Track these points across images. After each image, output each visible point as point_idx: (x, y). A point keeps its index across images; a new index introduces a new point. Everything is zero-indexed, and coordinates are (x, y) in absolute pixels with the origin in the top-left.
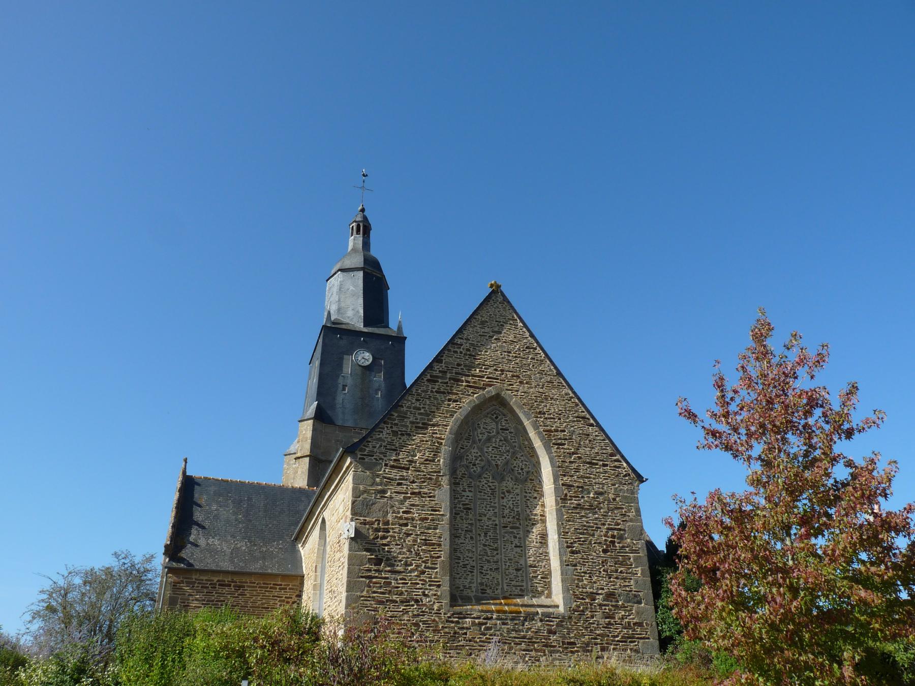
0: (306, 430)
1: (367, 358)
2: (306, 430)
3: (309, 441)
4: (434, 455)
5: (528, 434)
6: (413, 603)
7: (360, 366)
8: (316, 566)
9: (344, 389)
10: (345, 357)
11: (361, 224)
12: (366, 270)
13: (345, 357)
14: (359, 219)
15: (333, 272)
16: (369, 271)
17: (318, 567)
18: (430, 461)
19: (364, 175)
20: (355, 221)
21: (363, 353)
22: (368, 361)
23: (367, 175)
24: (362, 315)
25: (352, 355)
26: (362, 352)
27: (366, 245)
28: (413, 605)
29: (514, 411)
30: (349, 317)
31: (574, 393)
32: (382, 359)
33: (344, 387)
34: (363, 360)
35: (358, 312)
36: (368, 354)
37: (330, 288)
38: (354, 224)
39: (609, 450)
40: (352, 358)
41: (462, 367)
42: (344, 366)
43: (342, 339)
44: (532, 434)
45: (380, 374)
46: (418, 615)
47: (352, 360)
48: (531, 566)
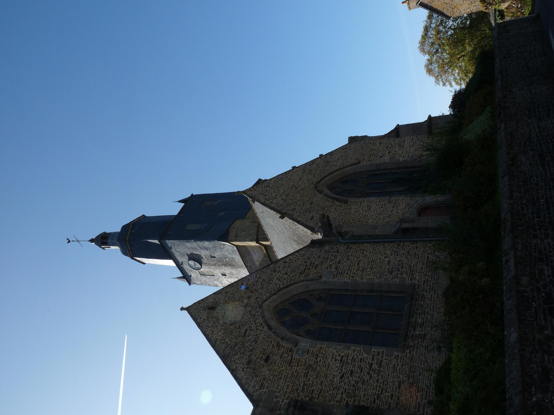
11: (103, 247)
12: (132, 255)
16: (131, 253)
20: (104, 249)
21: (191, 265)
23: (68, 239)
26: (191, 266)
43: (191, 275)
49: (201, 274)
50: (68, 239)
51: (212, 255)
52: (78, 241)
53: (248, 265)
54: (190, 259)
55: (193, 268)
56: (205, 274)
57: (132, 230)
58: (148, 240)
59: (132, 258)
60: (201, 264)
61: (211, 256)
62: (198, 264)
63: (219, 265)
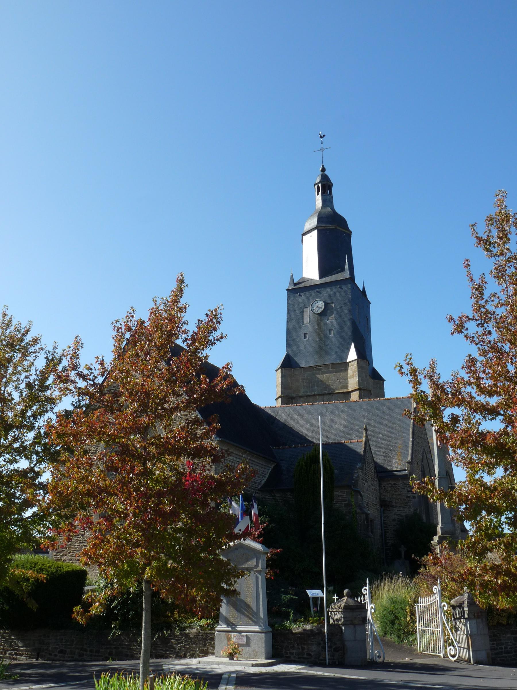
1: (320, 306)
4: (97, 449)
6: (81, 536)
9: (305, 337)
11: (320, 185)
12: (319, 228)
14: (318, 180)
18: (94, 453)
19: (321, 137)
20: (315, 184)
21: (317, 302)
22: (321, 308)
23: (324, 136)
26: (316, 302)
27: (327, 200)
28: (80, 537)
32: (332, 303)
34: (318, 308)
36: (321, 302)
41: (116, 388)
43: (301, 296)
45: (332, 317)
46: (83, 542)
49: (304, 309)
50: (324, 136)
51: (332, 332)
52: (322, 149)
53: (321, 367)
54: (326, 304)
55: (314, 304)
56: (304, 313)
57: (345, 233)
58: (347, 263)
59: (316, 228)
60: (320, 314)
61: (332, 330)
62: (320, 312)
63: (319, 334)
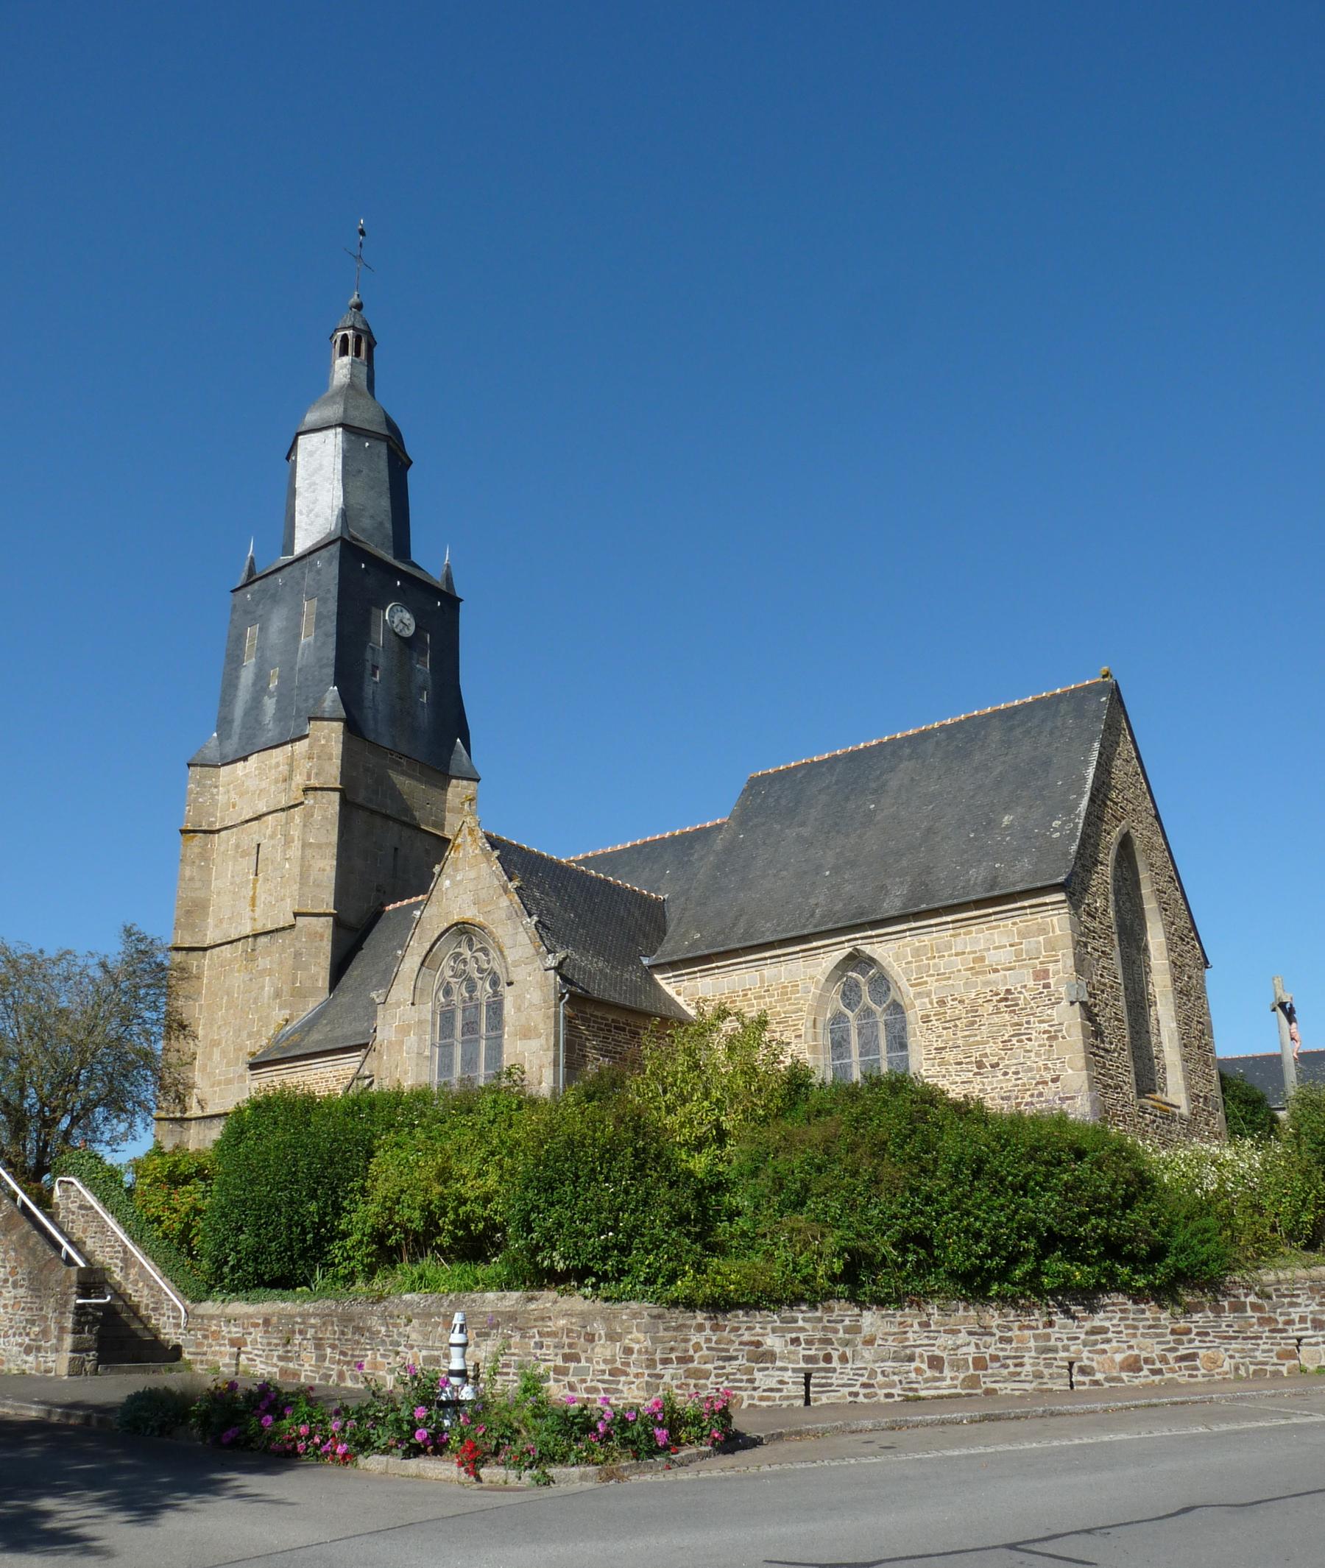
0: (328, 739)
1: (407, 622)
2: (328, 739)
3: (337, 762)
5: (1140, 890)
7: (396, 634)
8: (815, 1020)
10: (374, 610)
13: (374, 610)
15: (311, 418)
17: (818, 1021)
24: (391, 533)
25: (385, 611)
26: (399, 608)
29: (1134, 857)
30: (364, 530)
31: (1167, 844)
32: (427, 632)
33: (375, 668)
34: (401, 625)
35: (381, 524)
36: (407, 616)
37: (311, 454)
38: (350, 333)
39: (1189, 926)
40: (384, 616)
42: (373, 628)
44: (1146, 891)
47: (385, 620)
48: (1157, 1058)
